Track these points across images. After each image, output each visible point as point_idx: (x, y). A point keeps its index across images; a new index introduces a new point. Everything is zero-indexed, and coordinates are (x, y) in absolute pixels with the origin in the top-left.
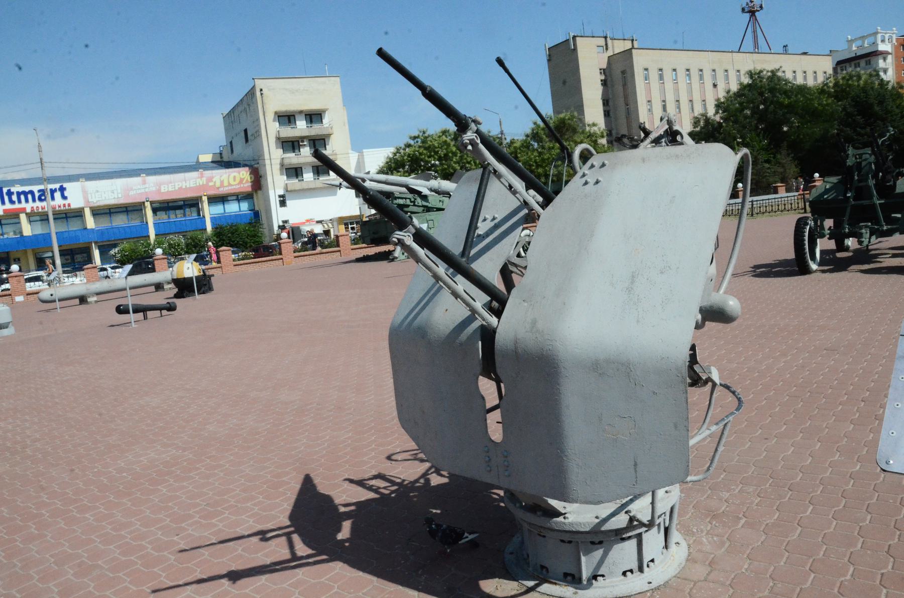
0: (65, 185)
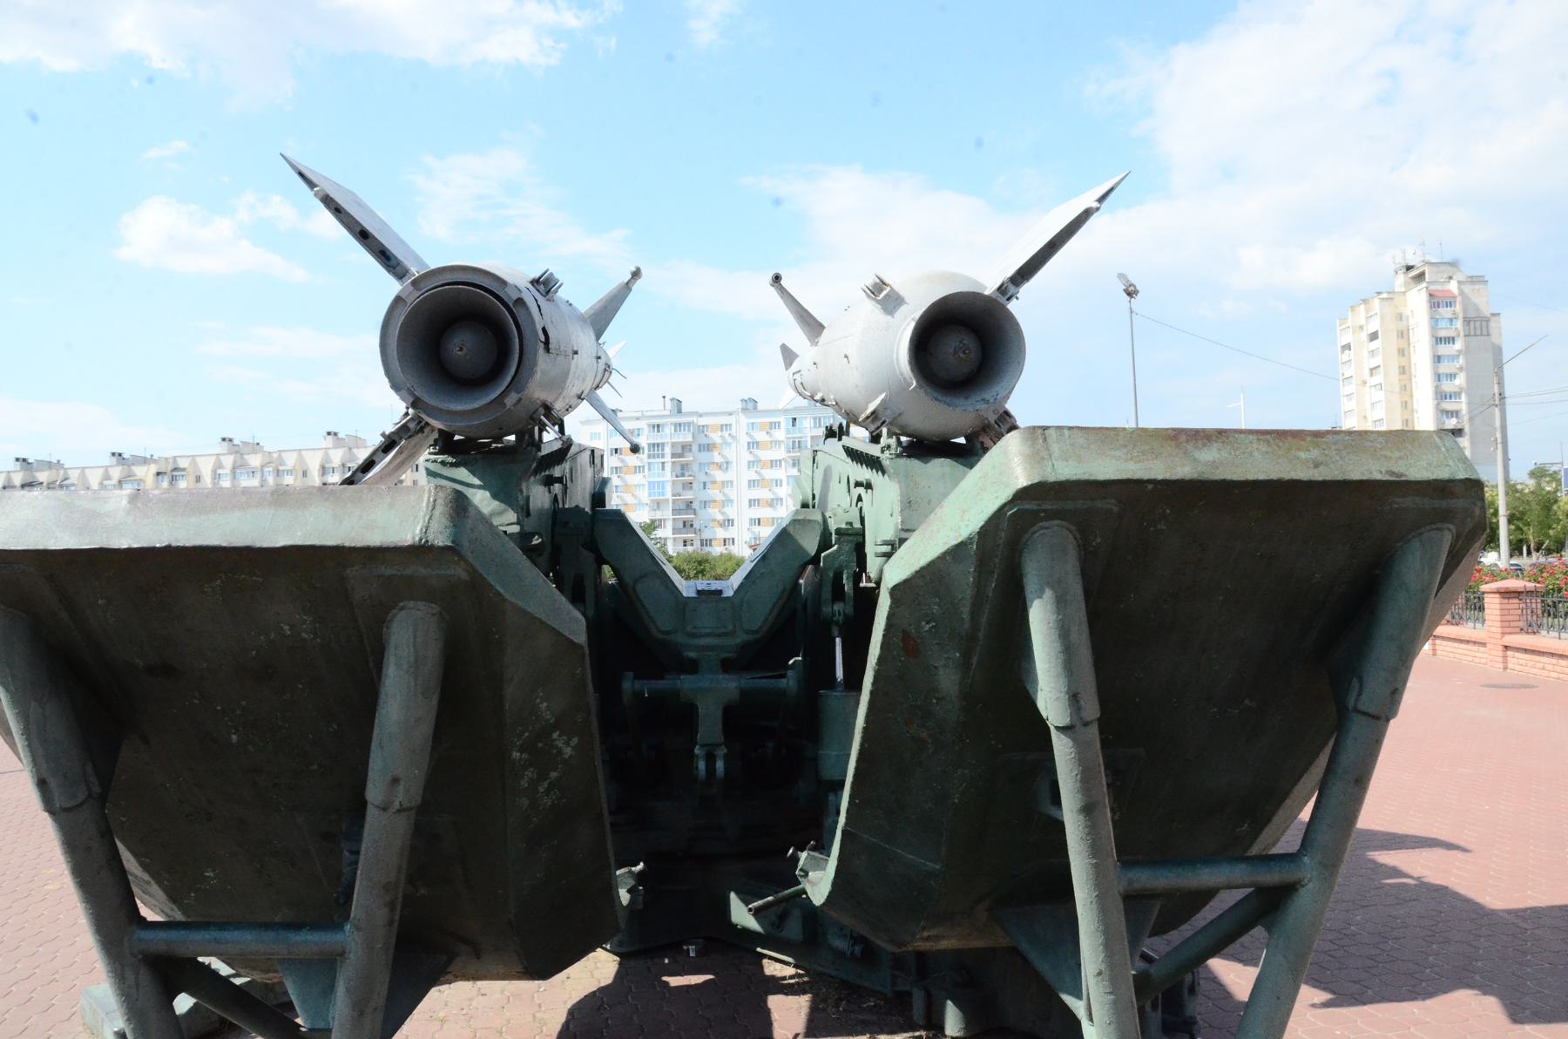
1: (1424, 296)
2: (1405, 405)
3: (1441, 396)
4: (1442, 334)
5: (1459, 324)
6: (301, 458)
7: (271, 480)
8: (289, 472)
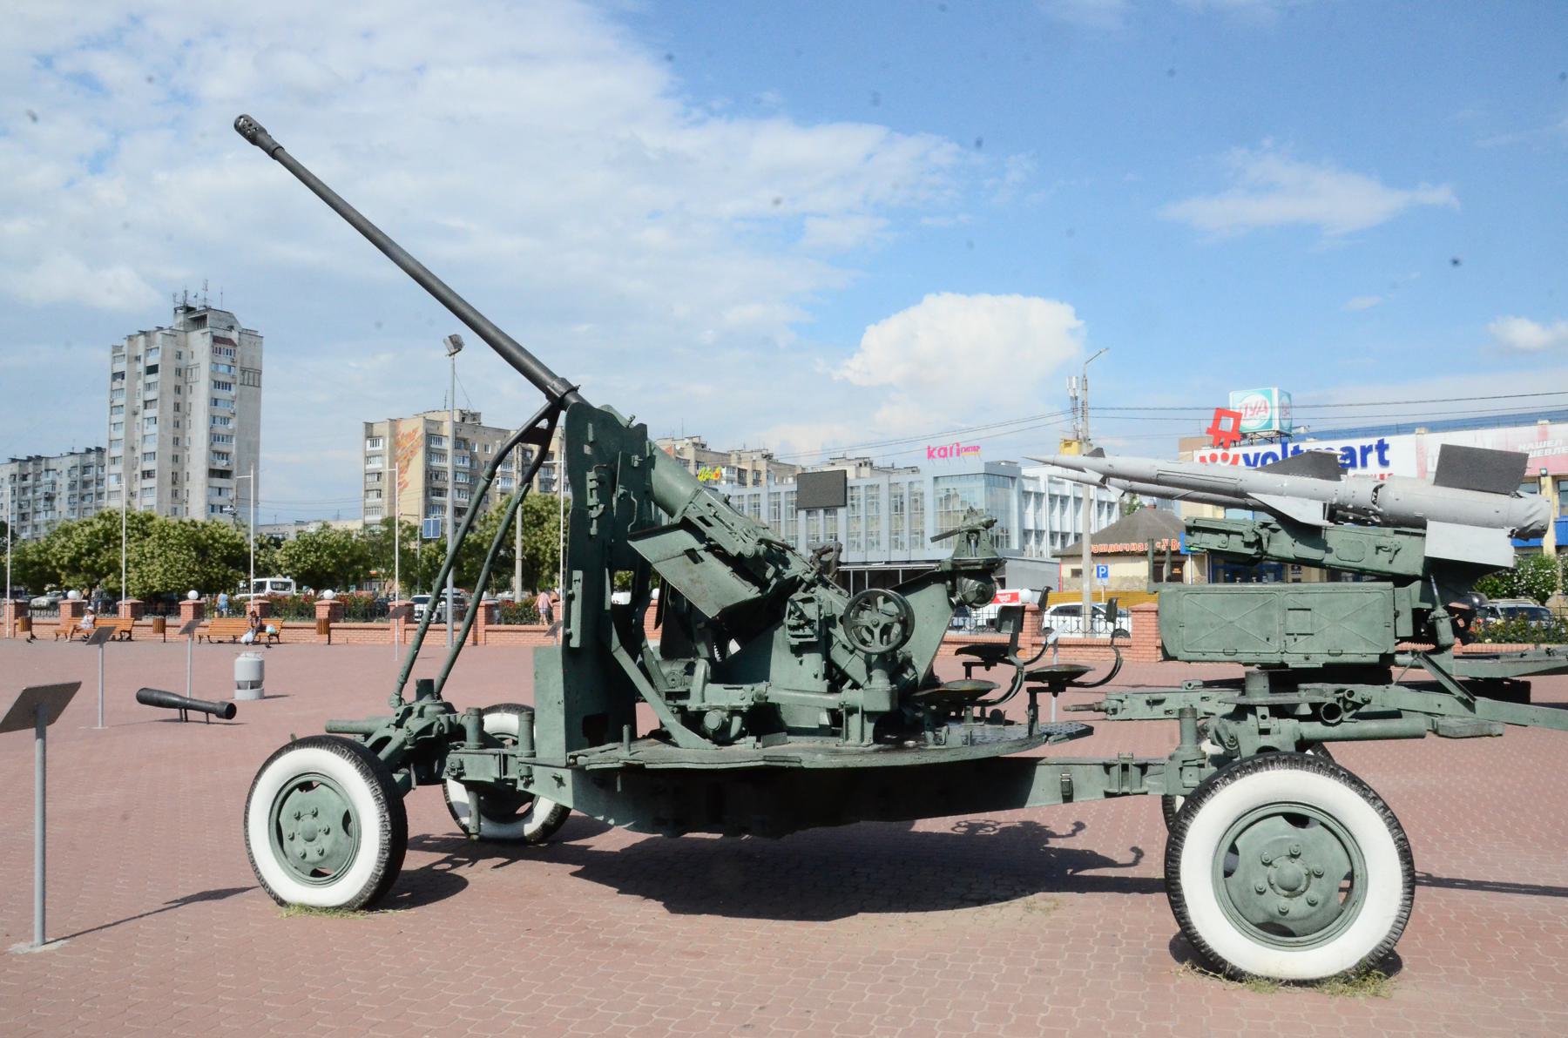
0: (1387, 440)
1: (208, 340)
2: (176, 441)
3: (214, 438)
4: (221, 379)
5: (236, 371)
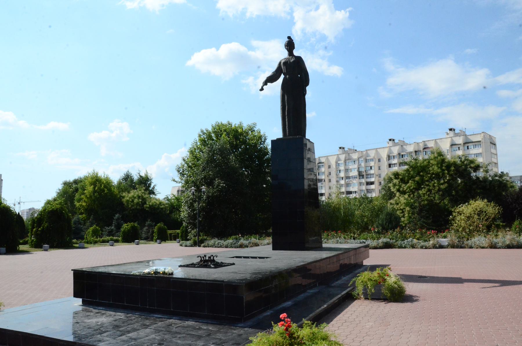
6: (377, 153)
7: (363, 164)
8: (372, 160)
